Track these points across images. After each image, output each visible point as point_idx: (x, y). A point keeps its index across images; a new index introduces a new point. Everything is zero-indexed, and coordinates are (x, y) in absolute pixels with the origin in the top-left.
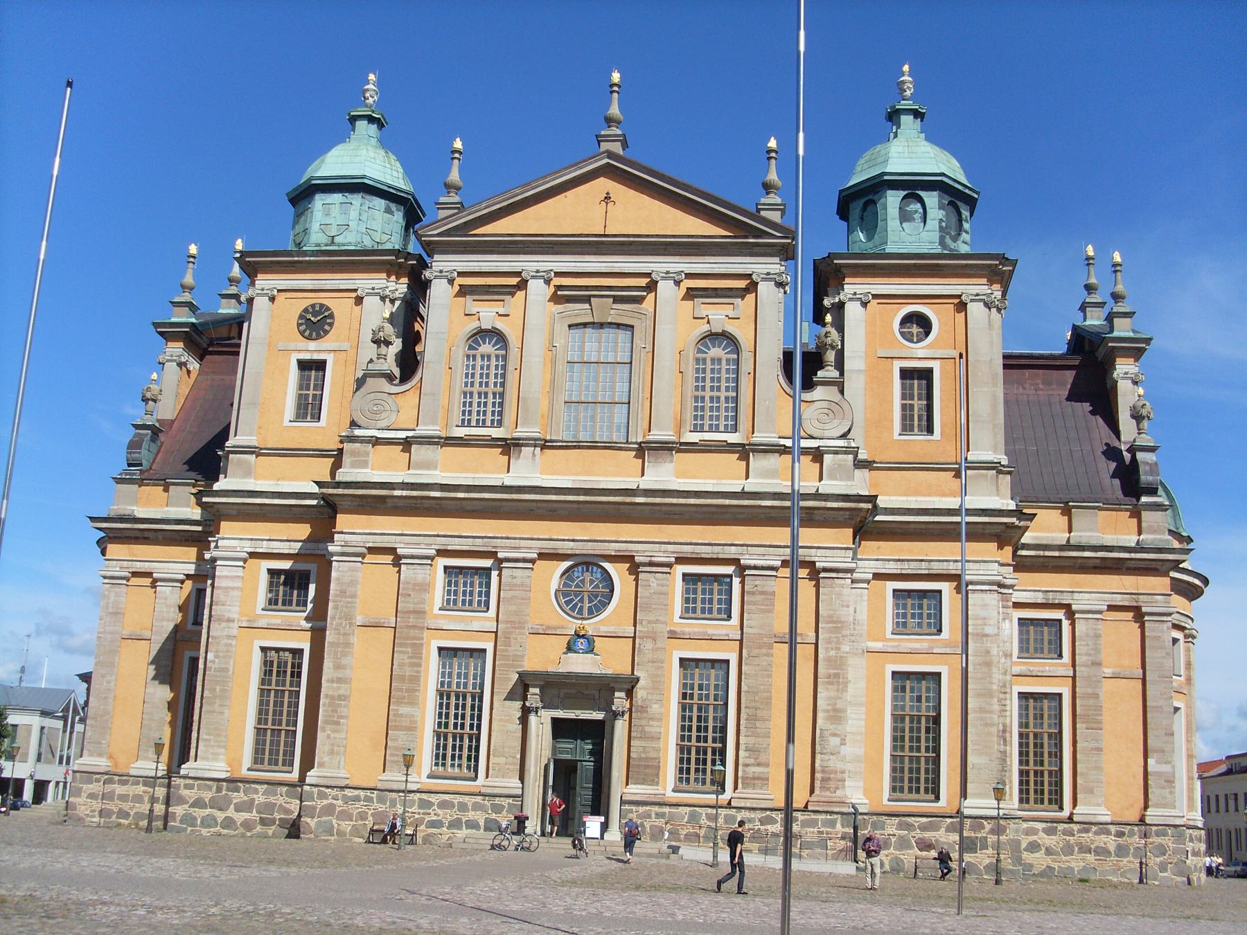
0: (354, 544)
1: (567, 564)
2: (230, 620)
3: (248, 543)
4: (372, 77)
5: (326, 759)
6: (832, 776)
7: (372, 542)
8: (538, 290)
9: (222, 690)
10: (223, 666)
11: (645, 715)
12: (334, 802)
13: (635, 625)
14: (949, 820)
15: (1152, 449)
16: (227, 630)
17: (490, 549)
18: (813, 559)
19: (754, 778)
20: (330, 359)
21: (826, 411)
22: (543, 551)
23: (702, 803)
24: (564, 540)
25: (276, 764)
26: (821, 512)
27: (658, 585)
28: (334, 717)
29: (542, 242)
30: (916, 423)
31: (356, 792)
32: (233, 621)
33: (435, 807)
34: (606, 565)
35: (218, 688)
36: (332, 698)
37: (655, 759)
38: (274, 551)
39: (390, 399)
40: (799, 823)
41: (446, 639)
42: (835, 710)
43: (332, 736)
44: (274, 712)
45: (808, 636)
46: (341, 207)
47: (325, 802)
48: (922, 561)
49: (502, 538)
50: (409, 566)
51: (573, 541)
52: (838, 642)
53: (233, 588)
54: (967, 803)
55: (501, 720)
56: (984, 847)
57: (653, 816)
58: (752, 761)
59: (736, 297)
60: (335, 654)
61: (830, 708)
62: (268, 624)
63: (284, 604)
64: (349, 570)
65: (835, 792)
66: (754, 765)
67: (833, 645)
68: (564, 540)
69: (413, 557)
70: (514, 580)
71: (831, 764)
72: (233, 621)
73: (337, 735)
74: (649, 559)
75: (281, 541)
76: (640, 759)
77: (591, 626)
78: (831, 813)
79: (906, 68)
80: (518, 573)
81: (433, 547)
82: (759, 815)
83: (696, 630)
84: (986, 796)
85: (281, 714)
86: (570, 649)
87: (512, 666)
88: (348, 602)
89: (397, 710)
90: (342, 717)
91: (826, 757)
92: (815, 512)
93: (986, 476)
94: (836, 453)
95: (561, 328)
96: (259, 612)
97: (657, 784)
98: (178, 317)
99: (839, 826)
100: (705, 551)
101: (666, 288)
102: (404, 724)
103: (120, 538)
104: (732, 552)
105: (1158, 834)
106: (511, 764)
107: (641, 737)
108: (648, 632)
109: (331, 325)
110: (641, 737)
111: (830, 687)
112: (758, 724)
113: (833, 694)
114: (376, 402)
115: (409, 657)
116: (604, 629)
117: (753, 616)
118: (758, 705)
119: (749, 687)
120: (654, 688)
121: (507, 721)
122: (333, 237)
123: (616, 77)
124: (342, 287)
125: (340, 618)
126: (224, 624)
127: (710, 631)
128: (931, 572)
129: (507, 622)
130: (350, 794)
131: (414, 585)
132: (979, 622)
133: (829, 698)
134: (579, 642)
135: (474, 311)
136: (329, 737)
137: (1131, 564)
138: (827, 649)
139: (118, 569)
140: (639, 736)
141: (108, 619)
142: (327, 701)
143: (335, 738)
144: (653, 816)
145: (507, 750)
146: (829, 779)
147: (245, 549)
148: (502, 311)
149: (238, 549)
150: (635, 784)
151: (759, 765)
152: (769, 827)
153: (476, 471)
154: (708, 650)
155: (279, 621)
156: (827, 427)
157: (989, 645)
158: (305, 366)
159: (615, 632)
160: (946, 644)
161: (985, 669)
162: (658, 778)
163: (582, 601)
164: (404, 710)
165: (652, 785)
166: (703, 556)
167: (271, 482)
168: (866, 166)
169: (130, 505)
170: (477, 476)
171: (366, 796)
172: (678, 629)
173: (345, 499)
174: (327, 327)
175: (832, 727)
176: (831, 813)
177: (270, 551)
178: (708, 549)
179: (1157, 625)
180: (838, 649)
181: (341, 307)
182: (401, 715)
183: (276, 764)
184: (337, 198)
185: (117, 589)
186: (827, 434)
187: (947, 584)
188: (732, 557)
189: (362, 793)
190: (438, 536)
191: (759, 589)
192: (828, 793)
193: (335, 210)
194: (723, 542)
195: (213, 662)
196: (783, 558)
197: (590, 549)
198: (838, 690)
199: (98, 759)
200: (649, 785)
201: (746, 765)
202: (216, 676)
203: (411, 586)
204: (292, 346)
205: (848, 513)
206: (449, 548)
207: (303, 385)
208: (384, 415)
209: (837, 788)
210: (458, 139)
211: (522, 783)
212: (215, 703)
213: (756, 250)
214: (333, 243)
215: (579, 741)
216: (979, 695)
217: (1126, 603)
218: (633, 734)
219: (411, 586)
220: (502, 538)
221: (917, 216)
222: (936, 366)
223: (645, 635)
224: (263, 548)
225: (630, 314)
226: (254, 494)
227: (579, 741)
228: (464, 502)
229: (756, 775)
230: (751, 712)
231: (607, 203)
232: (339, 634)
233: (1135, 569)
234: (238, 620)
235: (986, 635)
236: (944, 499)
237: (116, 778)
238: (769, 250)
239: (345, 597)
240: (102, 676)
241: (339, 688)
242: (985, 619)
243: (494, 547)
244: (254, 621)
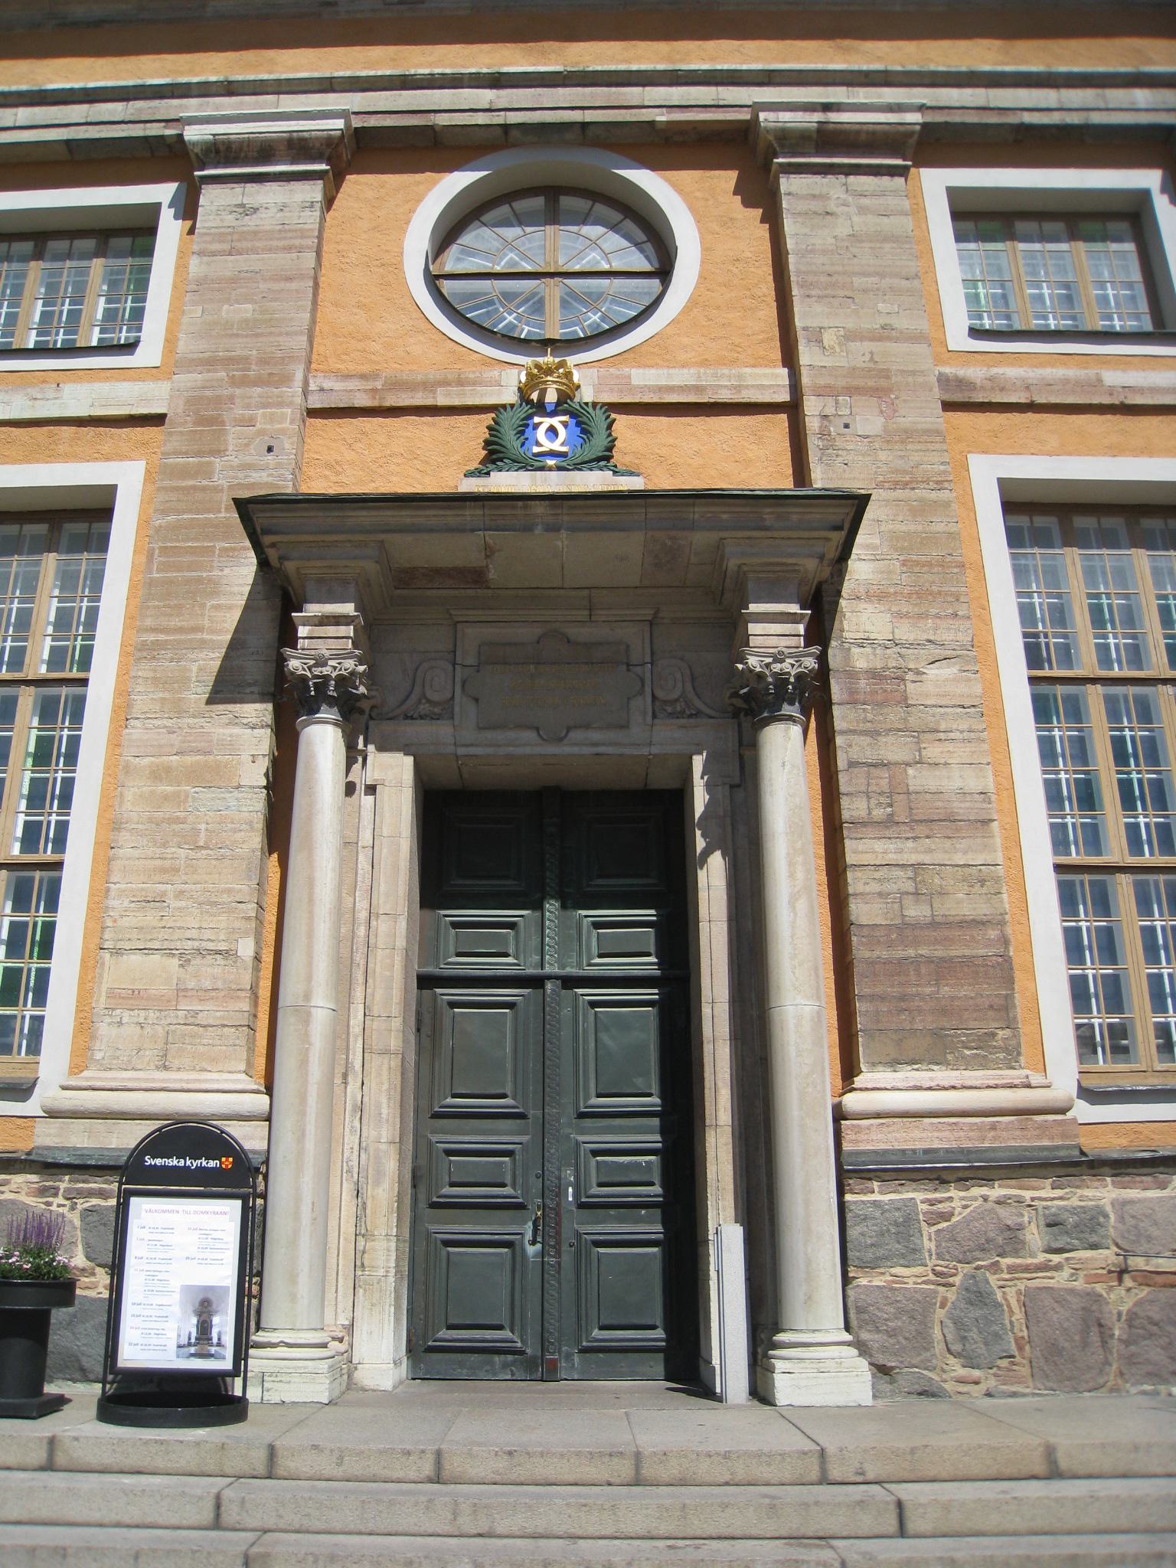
11: (893, 715)
13: (789, 357)
34: (646, 180)
37: (980, 923)
55: (158, 774)
70: (251, 222)
76: (905, 930)
97: (1012, 1056)
106: (204, 994)
107: (890, 822)
110: (890, 822)
120: (921, 594)
121: (198, 776)
127: (1113, 378)
129: (210, 363)
140: (879, 813)
144: (1034, 1236)
150: (894, 1063)
159: (698, 389)
162: (1011, 1024)
165: (983, 1064)
172: (974, 373)
200: (968, 1064)
211: (269, 1090)
215: (552, 906)
218: (851, 808)
223: (841, 383)
227: (552, 906)
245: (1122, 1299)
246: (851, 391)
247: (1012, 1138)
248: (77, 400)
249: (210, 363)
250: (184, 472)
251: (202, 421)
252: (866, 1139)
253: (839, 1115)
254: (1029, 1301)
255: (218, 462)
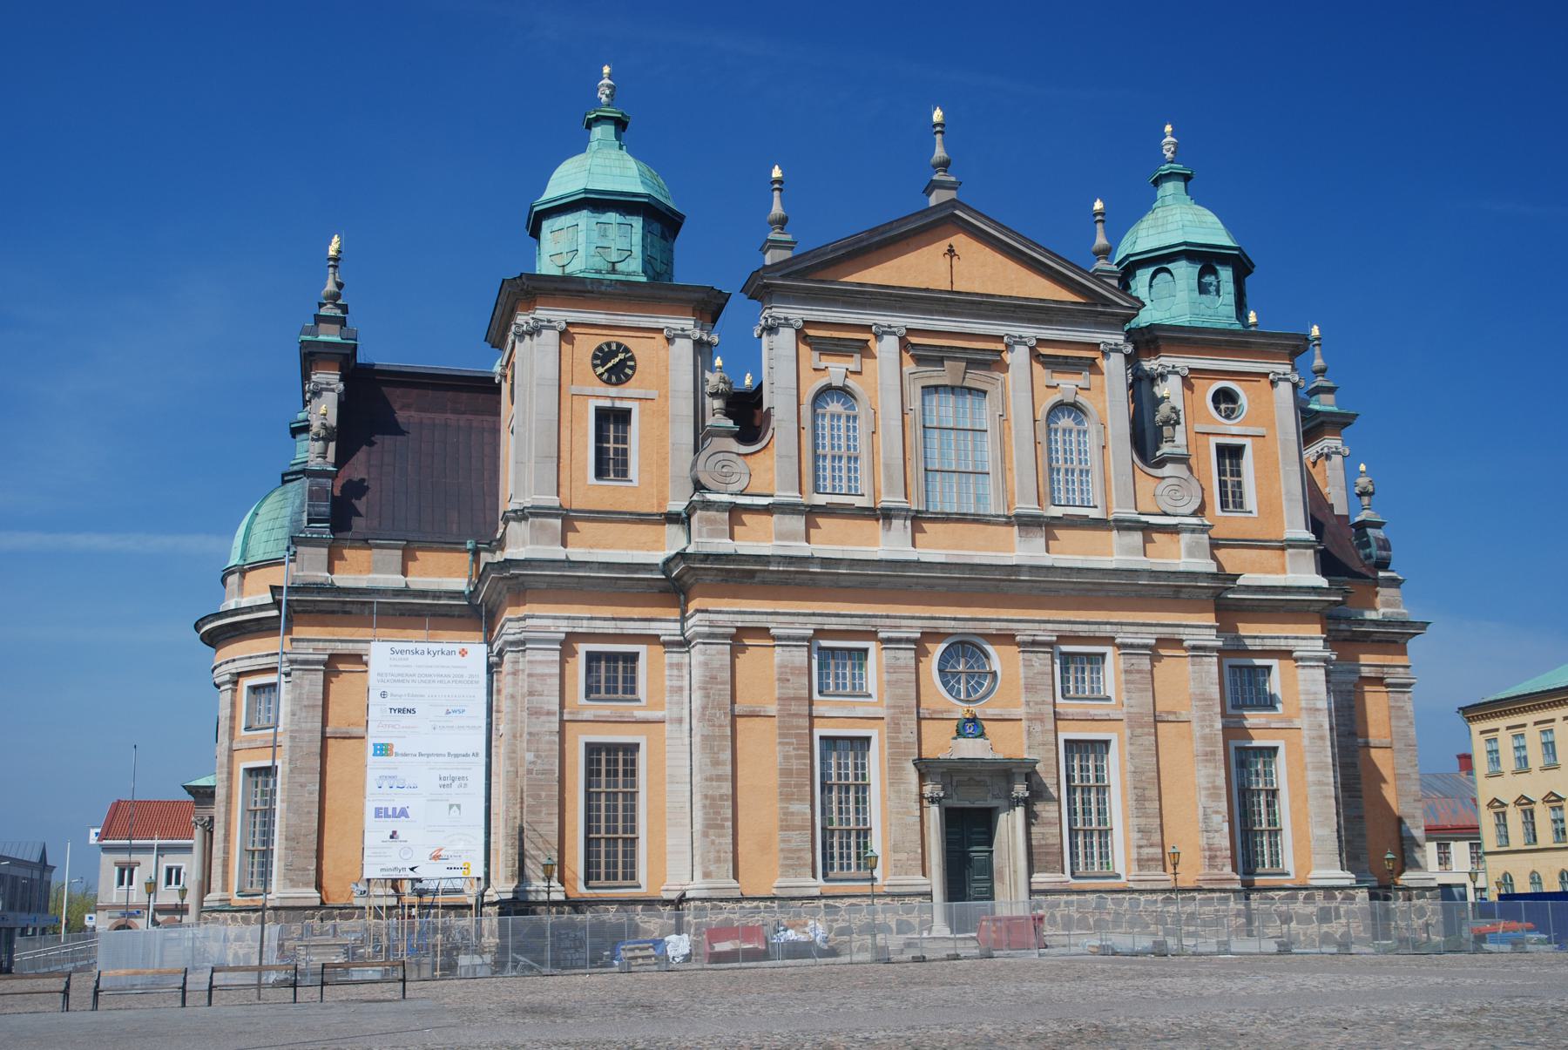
0: (720, 624)
1: (943, 646)
2: (549, 713)
3: (565, 623)
4: (606, 70)
5: (712, 868)
6: (1218, 853)
7: (742, 621)
8: (888, 347)
9: (547, 796)
10: (546, 767)
12: (731, 916)
14: (1305, 893)
15: (1378, 525)
16: (547, 725)
17: (869, 628)
18: (1181, 637)
19: (1148, 860)
20: (635, 407)
21: (1176, 488)
22: (925, 630)
23: (1108, 888)
24: (945, 619)
25: (615, 878)
26: (1189, 589)
27: (1041, 665)
28: (717, 819)
29: (891, 295)
30: (1230, 499)
31: (755, 904)
32: (554, 714)
33: (843, 913)
34: (989, 648)
35: (543, 794)
36: (713, 798)
38: (597, 631)
39: (740, 460)
40: (1197, 902)
41: (833, 727)
42: (1215, 787)
43: (717, 841)
44: (607, 819)
45: (1180, 714)
46: (620, 229)
47: (721, 917)
48: (1255, 637)
49: (882, 617)
50: (785, 649)
51: (955, 619)
52: (1211, 720)
53: (551, 675)
54: (1315, 873)
55: (898, 813)
56: (1338, 917)
57: (1062, 904)
58: (1144, 842)
59: (1085, 365)
60: (712, 748)
61: (1210, 785)
62: (595, 716)
63: (608, 691)
64: (718, 653)
65: (1222, 870)
66: (1146, 846)
67: (1208, 723)
68: (945, 619)
69: (788, 638)
70: (898, 662)
71: (1216, 841)
72: (554, 714)
73: (722, 840)
74: (1032, 638)
75: (605, 619)
76: (1041, 846)
77: (977, 710)
78: (1224, 891)
79: (1168, 128)
80: (901, 654)
81: (809, 626)
82: (1161, 897)
83: (1078, 710)
84: (1329, 866)
85: (616, 820)
86: (960, 733)
87: (906, 754)
88: (720, 690)
89: (787, 808)
90: (726, 819)
91: (1211, 835)
92: (1184, 590)
93: (1305, 554)
94: (1193, 531)
95: (915, 393)
96: (582, 700)
98: (328, 335)
99: (1232, 904)
100: (1082, 630)
101: (1018, 358)
102: (795, 823)
103: (311, 612)
104: (1107, 630)
105: (1419, 898)
106: (912, 860)
108: (1035, 714)
109: (633, 368)
111: (1208, 764)
112: (1147, 804)
113: (1212, 771)
114: (725, 463)
115: (798, 749)
116: (991, 712)
117: (1134, 695)
118: (1145, 785)
119: (1136, 768)
122: (614, 263)
123: (937, 115)
124: (642, 325)
125: (712, 708)
126: (543, 718)
127: (1092, 712)
128: (1265, 648)
129: (894, 707)
130: (748, 906)
131: (792, 668)
132: (1311, 697)
133: (1208, 776)
134: (971, 726)
135: (822, 365)
136: (713, 843)
137: (1376, 637)
138: (1202, 727)
139: (311, 651)
141: (304, 714)
142: (708, 802)
143: (720, 844)
144: (1062, 904)
145: (907, 844)
146: (1216, 857)
147: (562, 629)
148: (852, 367)
149: (552, 629)
151: (1151, 846)
152: (1170, 908)
153: (842, 543)
154: (1091, 731)
155: (607, 712)
156: (1179, 503)
157: (1321, 719)
158: (603, 416)
160: (1282, 719)
161: (1319, 743)
163: (958, 682)
164: (795, 807)
166: (1081, 634)
167: (582, 550)
168: (1152, 231)
169: (319, 570)
170: (845, 548)
171: (766, 907)
173: (709, 572)
174: (629, 371)
175: (1213, 804)
176: (1224, 891)
177: (592, 631)
178: (1086, 627)
179: (1400, 695)
180: (1212, 726)
181: (639, 347)
182: (792, 814)
183: (615, 878)
184: (612, 217)
185: (311, 676)
186: (1180, 511)
187: (1277, 661)
188: (1108, 635)
189: (762, 904)
190: (814, 614)
191: (1136, 667)
192: (1216, 871)
193: (613, 232)
194: (1154, 622)
195: (533, 763)
196: (1155, 636)
197: (970, 627)
198: (1216, 767)
199: (304, 890)
201: (1140, 847)
202: (541, 780)
203: (788, 670)
204: (588, 391)
205: (1211, 591)
206: (826, 627)
207: (600, 437)
208: (734, 478)
209: (1224, 865)
210: (777, 167)
212: (540, 812)
213: (1101, 318)
214: (614, 271)
216: (1317, 768)
217: (1373, 675)
219: (788, 670)
220: (882, 617)
221: (1212, 289)
222: (1247, 442)
224: (585, 626)
225: (983, 379)
226: (576, 565)
228: (842, 578)
229: (1150, 856)
230: (1139, 792)
231: (951, 257)
232: (714, 725)
233: (1379, 641)
234: (561, 714)
235: (1318, 710)
236: (1268, 576)
237: (336, 912)
238: (1112, 320)
239: (717, 684)
240: (301, 786)
241: (720, 787)
242: (1316, 693)
243: (873, 626)
244: (578, 713)
245: (1077, 916)
246: (1035, 719)
247: (1059, 887)
248: (860, 712)
249: (894, 707)
250: (893, 738)
251: (896, 724)
252: (1034, 887)
253: (1030, 883)
254: (1062, 916)
255: (900, 735)
